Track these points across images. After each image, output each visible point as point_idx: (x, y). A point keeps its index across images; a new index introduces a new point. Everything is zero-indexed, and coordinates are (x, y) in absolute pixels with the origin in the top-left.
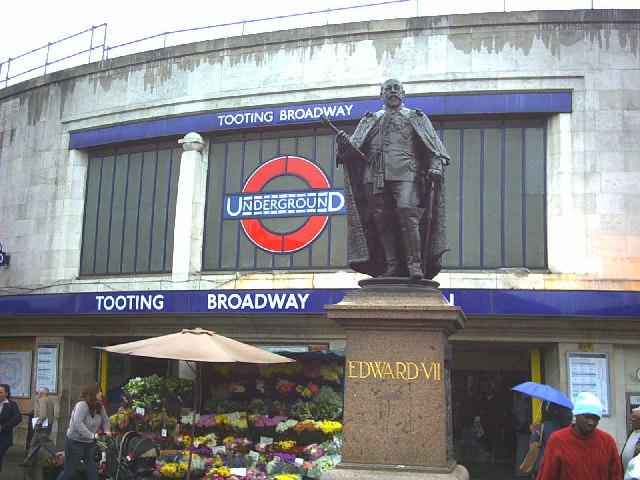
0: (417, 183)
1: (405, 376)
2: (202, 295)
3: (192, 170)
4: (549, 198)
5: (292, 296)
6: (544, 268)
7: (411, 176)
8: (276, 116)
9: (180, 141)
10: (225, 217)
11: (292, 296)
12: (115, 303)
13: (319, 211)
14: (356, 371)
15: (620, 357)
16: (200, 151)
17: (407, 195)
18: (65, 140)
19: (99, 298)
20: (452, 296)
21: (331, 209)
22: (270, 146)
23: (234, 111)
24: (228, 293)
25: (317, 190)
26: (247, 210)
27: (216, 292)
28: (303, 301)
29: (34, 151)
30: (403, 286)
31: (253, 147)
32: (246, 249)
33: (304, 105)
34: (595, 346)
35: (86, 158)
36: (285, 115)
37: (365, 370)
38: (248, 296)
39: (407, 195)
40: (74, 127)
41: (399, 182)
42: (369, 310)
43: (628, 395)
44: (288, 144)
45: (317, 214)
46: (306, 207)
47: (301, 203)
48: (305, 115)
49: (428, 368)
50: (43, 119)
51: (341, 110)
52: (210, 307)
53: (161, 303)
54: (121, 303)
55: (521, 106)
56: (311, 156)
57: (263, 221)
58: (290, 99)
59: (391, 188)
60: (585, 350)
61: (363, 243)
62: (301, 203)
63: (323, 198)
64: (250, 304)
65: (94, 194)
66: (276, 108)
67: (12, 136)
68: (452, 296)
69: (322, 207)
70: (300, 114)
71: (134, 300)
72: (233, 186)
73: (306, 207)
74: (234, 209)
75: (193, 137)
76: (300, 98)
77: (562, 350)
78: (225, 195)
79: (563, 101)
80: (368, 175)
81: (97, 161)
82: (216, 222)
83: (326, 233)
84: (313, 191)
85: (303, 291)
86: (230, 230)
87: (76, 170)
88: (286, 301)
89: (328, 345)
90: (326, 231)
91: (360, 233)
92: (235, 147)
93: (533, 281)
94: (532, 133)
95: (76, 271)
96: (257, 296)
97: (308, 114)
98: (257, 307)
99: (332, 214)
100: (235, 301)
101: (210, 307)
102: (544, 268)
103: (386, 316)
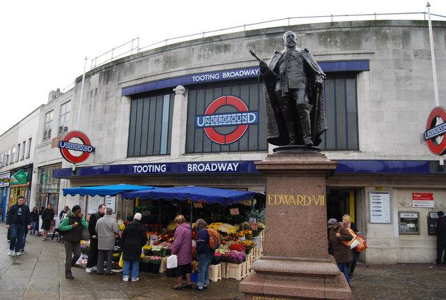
0: (307, 91)
1: (303, 203)
2: (184, 165)
3: (181, 100)
4: (359, 114)
5: (230, 165)
6: (357, 149)
7: (303, 86)
8: (221, 76)
9: (174, 90)
10: (197, 127)
11: (230, 165)
12: (142, 169)
13: (243, 122)
14: (272, 201)
15: (395, 192)
17: (302, 98)
18: (120, 92)
19: (135, 167)
21: (249, 122)
22: (218, 91)
23: (200, 74)
24: (198, 163)
25: (242, 112)
26: (207, 123)
27: (192, 163)
28: (236, 167)
29: (106, 98)
30: (301, 151)
31: (209, 93)
32: (208, 142)
33: (235, 70)
35: (130, 101)
36: (225, 76)
37: (278, 200)
38: (208, 165)
39: (302, 98)
40: (123, 85)
41: (297, 90)
42: (285, 165)
43: (399, 213)
44: (227, 90)
45: (242, 124)
46: (237, 121)
47: (234, 119)
48: (235, 75)
49: (317, 198)
50: (110, 82)
51: (253, 72)
52: (189, 170)
53: (165, 169)
54: (145, 169)
55: (344, 68)
56: (238, 95)
57: (216, 129)
58: (227, 67)
59: (292, 93)
60: (378, 190)
61: (275, 125)
62: (234, 119)
63: (245, 116)
64: (209, 169)
65: (134, 117)
66: (221, 72)
67: (96, 91)
69: (244, 120)
71: (152, 168)
72: (200, 111)
73: (237, 121)
75: (181, 87)
76: (232, 67)
77: (366, 191)
78: (196, 116)
79: (364, 66)
80: (278, 87)
81: (135, 102)
82: (191, 129)
83: (247, 134)
84: (239, 113)
85: (236, 162)
86: (199, 133)
87: (125, 105)
88: (227, 166)
89: (248, 189)
90: (247, 134)
91: (274, 120)
92: (201, 93)
93: (352, 156)
94: (349, 82)
95: (125, 154)
96: (212, 165)
97: (237, 74)
98: (213, 170)
99: (250, 124)
100: (201, 167)
101: (189, 170)
102: (357, 149)
103: (292, 168)
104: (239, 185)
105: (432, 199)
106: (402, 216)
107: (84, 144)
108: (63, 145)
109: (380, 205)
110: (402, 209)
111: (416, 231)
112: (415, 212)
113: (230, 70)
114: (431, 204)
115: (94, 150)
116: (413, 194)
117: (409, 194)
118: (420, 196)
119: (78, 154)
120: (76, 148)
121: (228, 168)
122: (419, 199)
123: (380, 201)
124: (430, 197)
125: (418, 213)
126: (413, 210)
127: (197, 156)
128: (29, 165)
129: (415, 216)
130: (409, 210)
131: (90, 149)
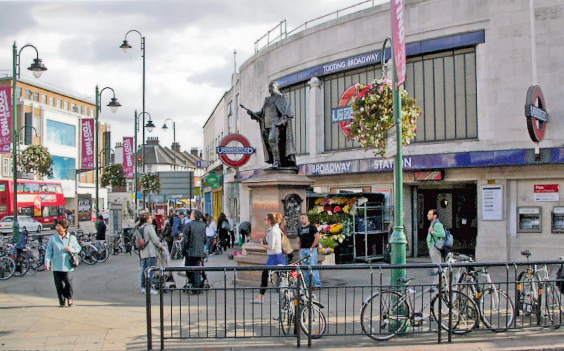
6: (475, 138)
11: (344, 164)
15: (513, 185)
16: (320, 87)
20: (410, 159)
33: (358, 56)
34: (496, 181)
43: (518, 209)
55: (458, 42)
66: (345, 60)
68: (410, 159)
70: (356, 61)
72: (335, 105)
74: (336, 118)
76: (355, 53)
79: (481, 36)
102: (475, 138)
104: (362, 183)
105: (557, 190)
106: (522, 211)
107: (245, 147)
108: (220, 151)
109: (491, 200)
110: (521, 204)
111: (537, 229)
112: (536, 207)
113: (353, 57)
114: (554, 196)
115: (255, 151)
116: (535, 186)
117: (530, 186)
118: (542, 188)
119: (239, 157)
120: (235, 151)
121: (343, 168)
122: (541, 191)
123: (492, 197)
124: (554, 188)
125: (540, 209)
126: (536, 204)
127: (330, 154)
128: (219, 166)
129: (536, 211)
130: (530, 204)
131: (250, 151)
